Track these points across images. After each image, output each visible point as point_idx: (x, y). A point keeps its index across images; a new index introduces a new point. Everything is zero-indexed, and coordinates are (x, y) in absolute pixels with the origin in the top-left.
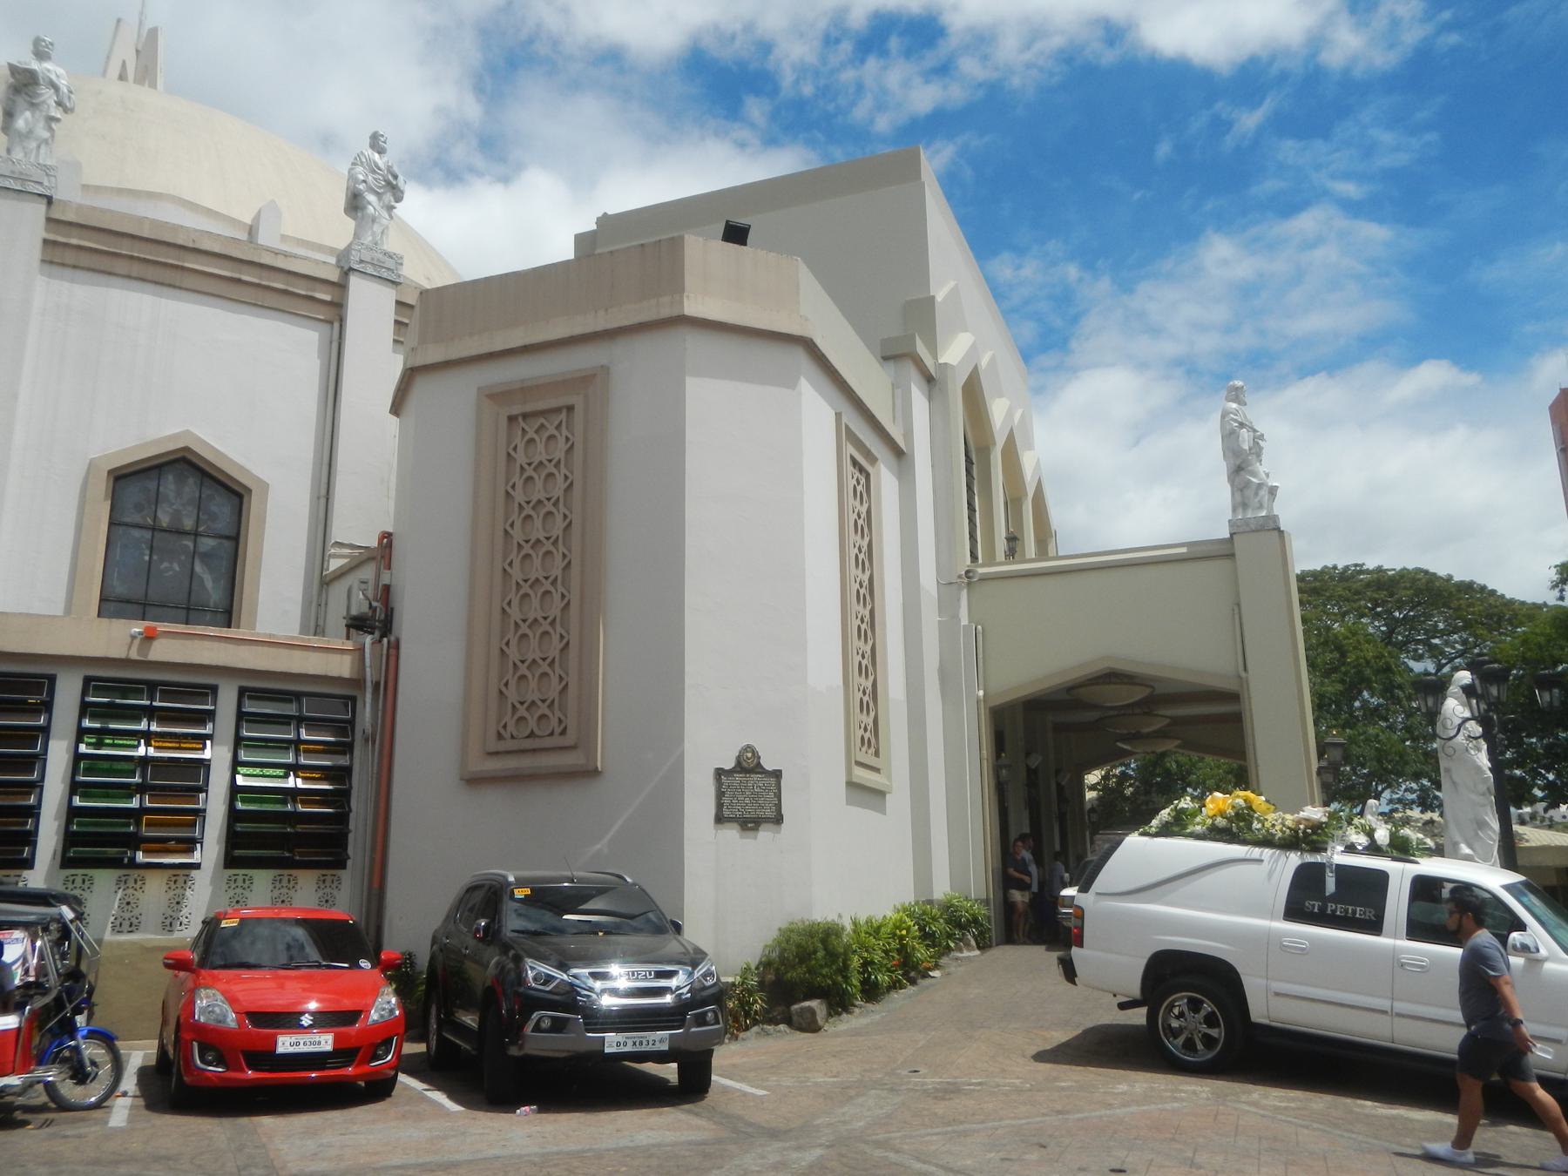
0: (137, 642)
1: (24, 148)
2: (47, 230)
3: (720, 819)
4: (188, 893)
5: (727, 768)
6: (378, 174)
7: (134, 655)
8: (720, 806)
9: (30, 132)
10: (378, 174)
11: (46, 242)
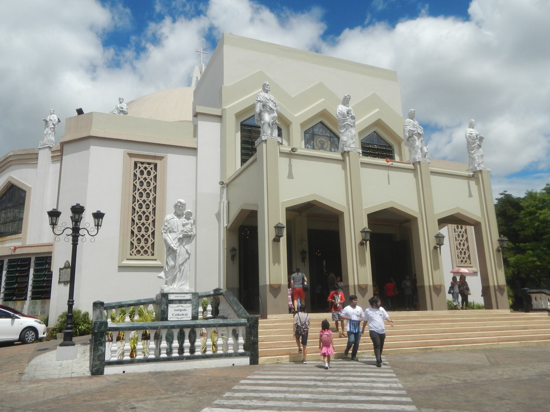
0: (13, 250)
1: (47, 137)
2: (52, 154)
3: (59, 282)
4: (25, 306)
5: (62, 267)
6: (118, 109)
7: (13, 254)
8: (60, 278)
9: (48, 133)
10: (118, 109)
11: (52, 157)
